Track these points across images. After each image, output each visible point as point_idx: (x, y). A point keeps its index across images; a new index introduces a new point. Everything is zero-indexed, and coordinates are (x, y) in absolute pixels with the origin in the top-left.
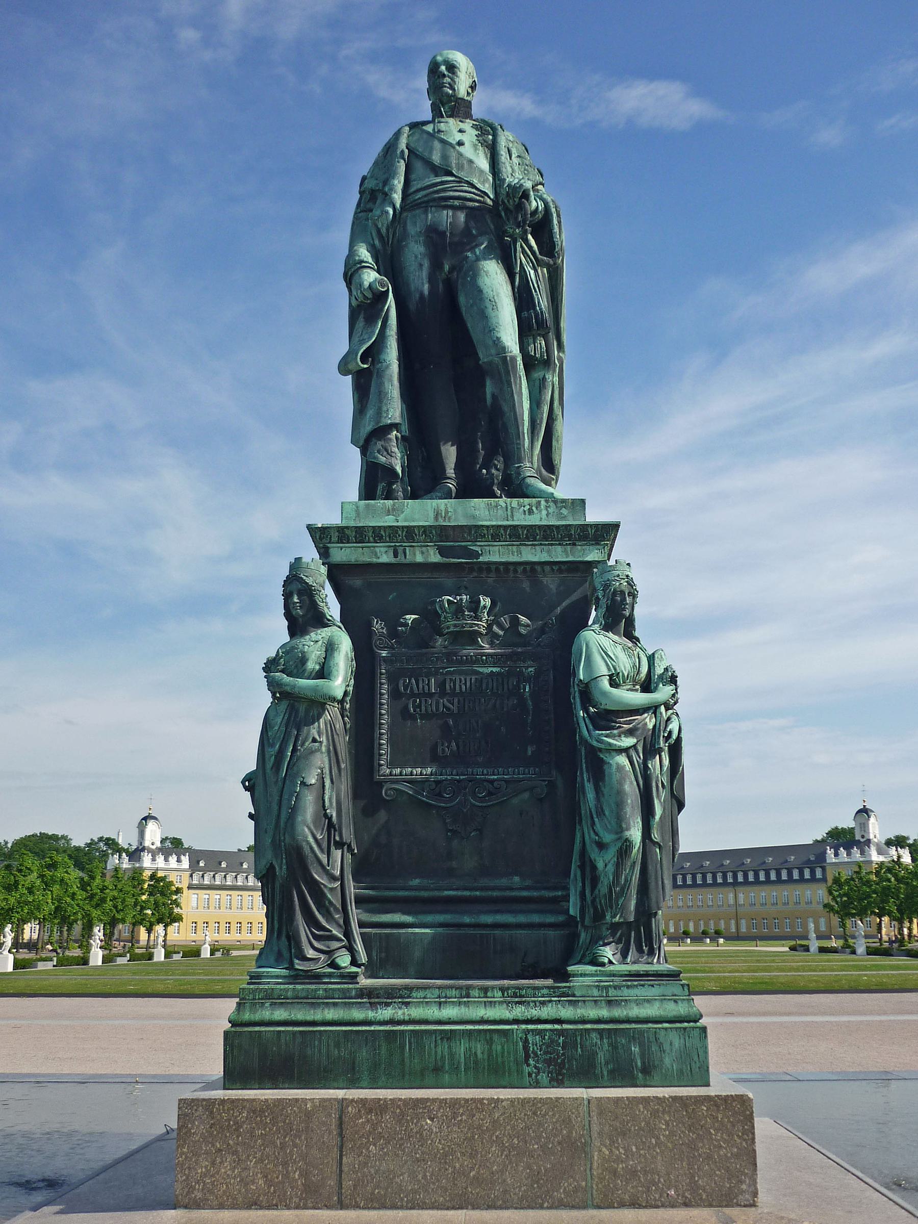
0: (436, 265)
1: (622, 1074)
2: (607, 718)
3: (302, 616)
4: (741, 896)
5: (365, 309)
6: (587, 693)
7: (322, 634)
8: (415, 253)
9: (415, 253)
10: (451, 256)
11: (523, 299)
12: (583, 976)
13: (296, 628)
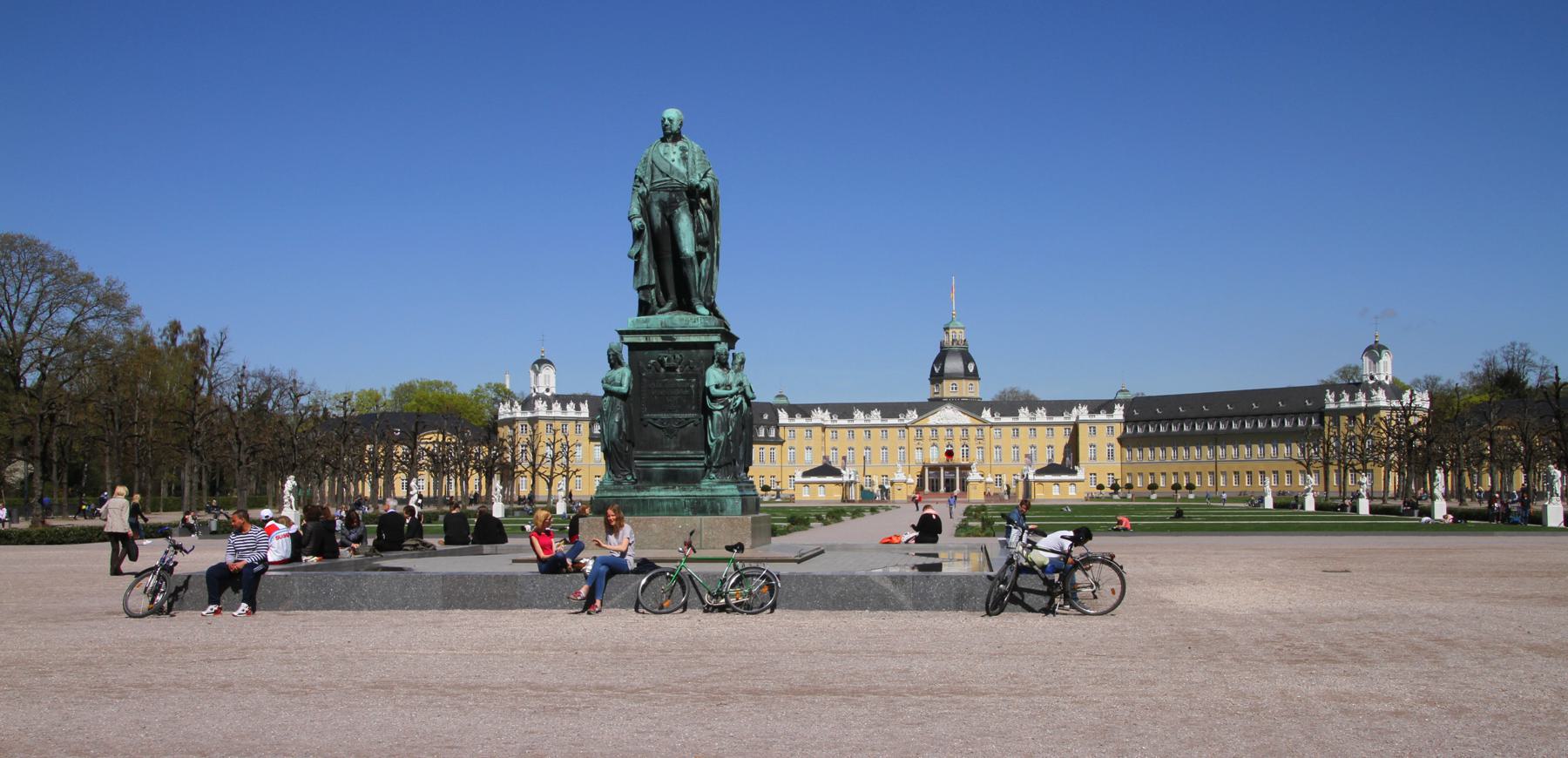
0: (664, 215)
1: (715, 512)
2: (714, 399)
3: (615, 362)
4: (1220, 451)
5: (638, 235)
6: (707, 390)
7: (620, 370)
8: (656, 209)
9: (656, 209)
10: (669, 210)
11: (697, 228)
12: (705, 483)
13: (613, 366)
